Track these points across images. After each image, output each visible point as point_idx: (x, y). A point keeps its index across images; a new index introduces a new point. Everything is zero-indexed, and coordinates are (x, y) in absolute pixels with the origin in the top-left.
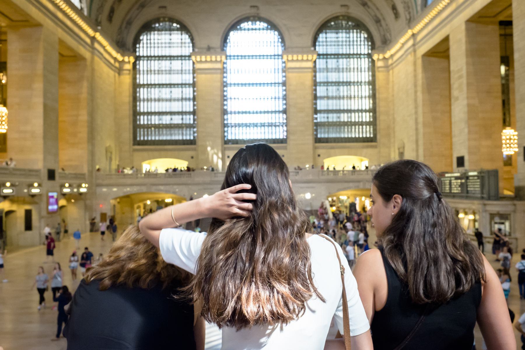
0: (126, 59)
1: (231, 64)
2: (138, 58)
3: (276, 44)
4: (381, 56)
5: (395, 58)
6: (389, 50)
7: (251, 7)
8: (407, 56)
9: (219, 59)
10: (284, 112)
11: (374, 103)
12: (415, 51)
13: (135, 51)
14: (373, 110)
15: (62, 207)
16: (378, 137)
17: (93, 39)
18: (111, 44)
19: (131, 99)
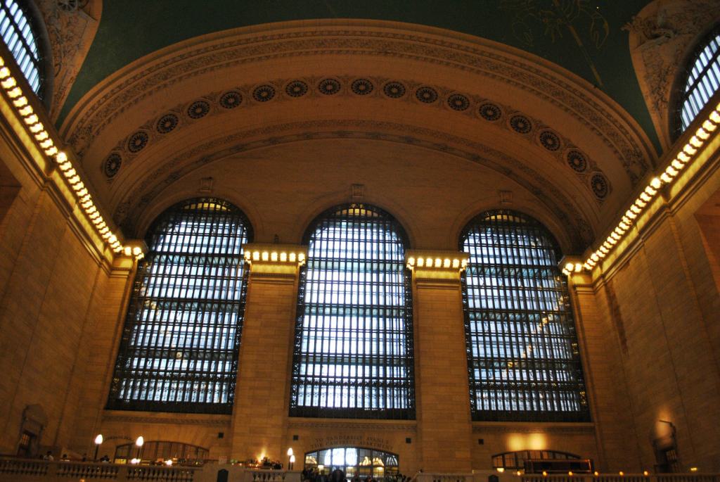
0: (128, 251)
5: (606, 265)
7: (354, 185)
8: (645, 239)
9: (292, 257)
13: (150, 244)
14: (576, 364)
16: (593, 411)
17: (52, 163)
18: (96, 200)
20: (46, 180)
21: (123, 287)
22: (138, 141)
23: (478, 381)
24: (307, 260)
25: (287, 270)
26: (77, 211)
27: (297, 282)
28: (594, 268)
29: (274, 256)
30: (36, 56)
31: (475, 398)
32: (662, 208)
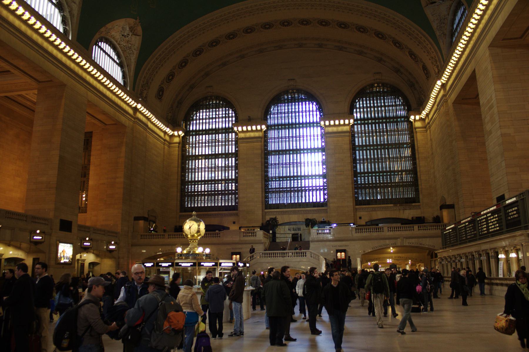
0: (176, 133)
1: (272, 134)
2: (188, 133)
3: (315, 113)
4: (417, 117)
5: (430, 116)
6: (424, 109)
9: (259, 127)
10: (324, 176)
11: (414, 164)
12: (446, 101)
13: (186, 127)
14: (414, 171)
15: (92, 264)
16: (421, 197)
17: (135, 109)
19: (180, 169)
20: (135, 118)
21: (177, 152)
22: (170, 77)
23: (359, 184)
24: (268, 127)
25: (257, 134)
26: (149, 124)
27: (263, 140)
28: (426, 117)
29: (249, 128)
30: (118, 61)
31: (357, 193)
32: (444, 96)
